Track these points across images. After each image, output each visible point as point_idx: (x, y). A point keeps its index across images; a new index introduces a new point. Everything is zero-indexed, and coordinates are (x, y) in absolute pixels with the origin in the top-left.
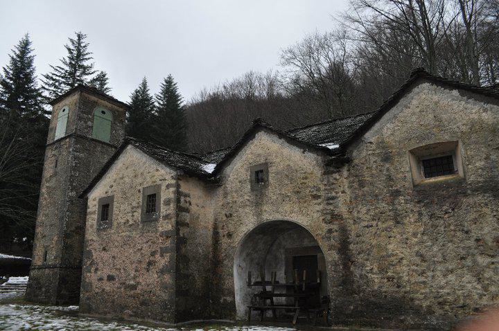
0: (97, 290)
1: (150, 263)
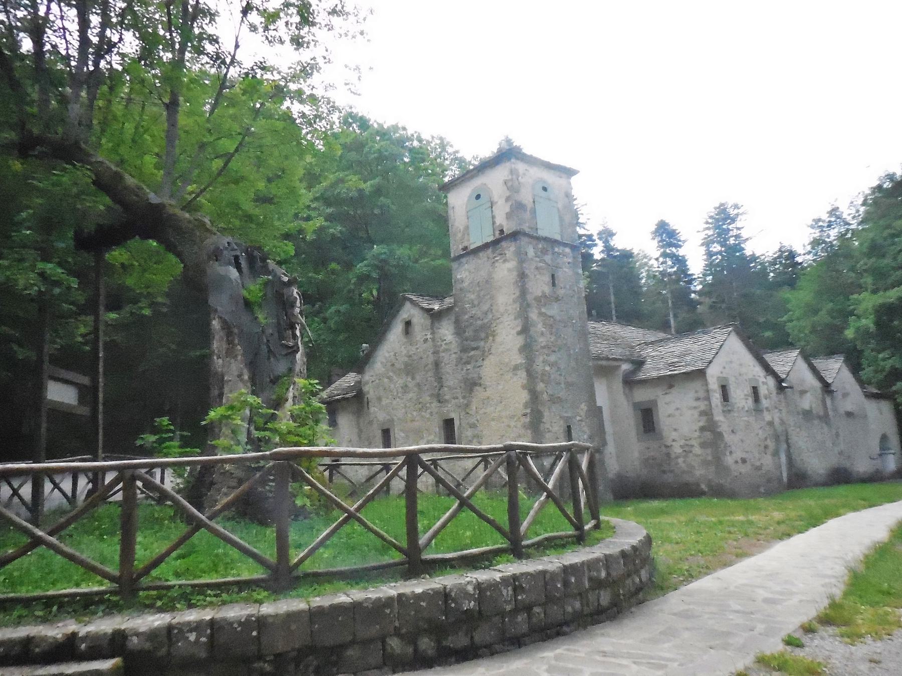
0: (736, 474)
1: (766, 447)
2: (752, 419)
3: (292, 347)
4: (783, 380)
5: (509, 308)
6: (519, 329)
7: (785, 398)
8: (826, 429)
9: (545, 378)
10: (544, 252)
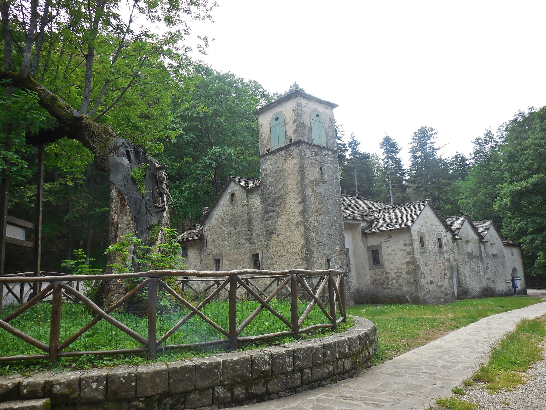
0: (427, 290)
1: (445, 274)
2: (437, 258)
3: (161, 208)
4: (456, 235)
5: (294, 187)
6: (300, 200)
7: (457, 245)
8: (481, 265)
9: (316, 230)
10: (316, 153)
